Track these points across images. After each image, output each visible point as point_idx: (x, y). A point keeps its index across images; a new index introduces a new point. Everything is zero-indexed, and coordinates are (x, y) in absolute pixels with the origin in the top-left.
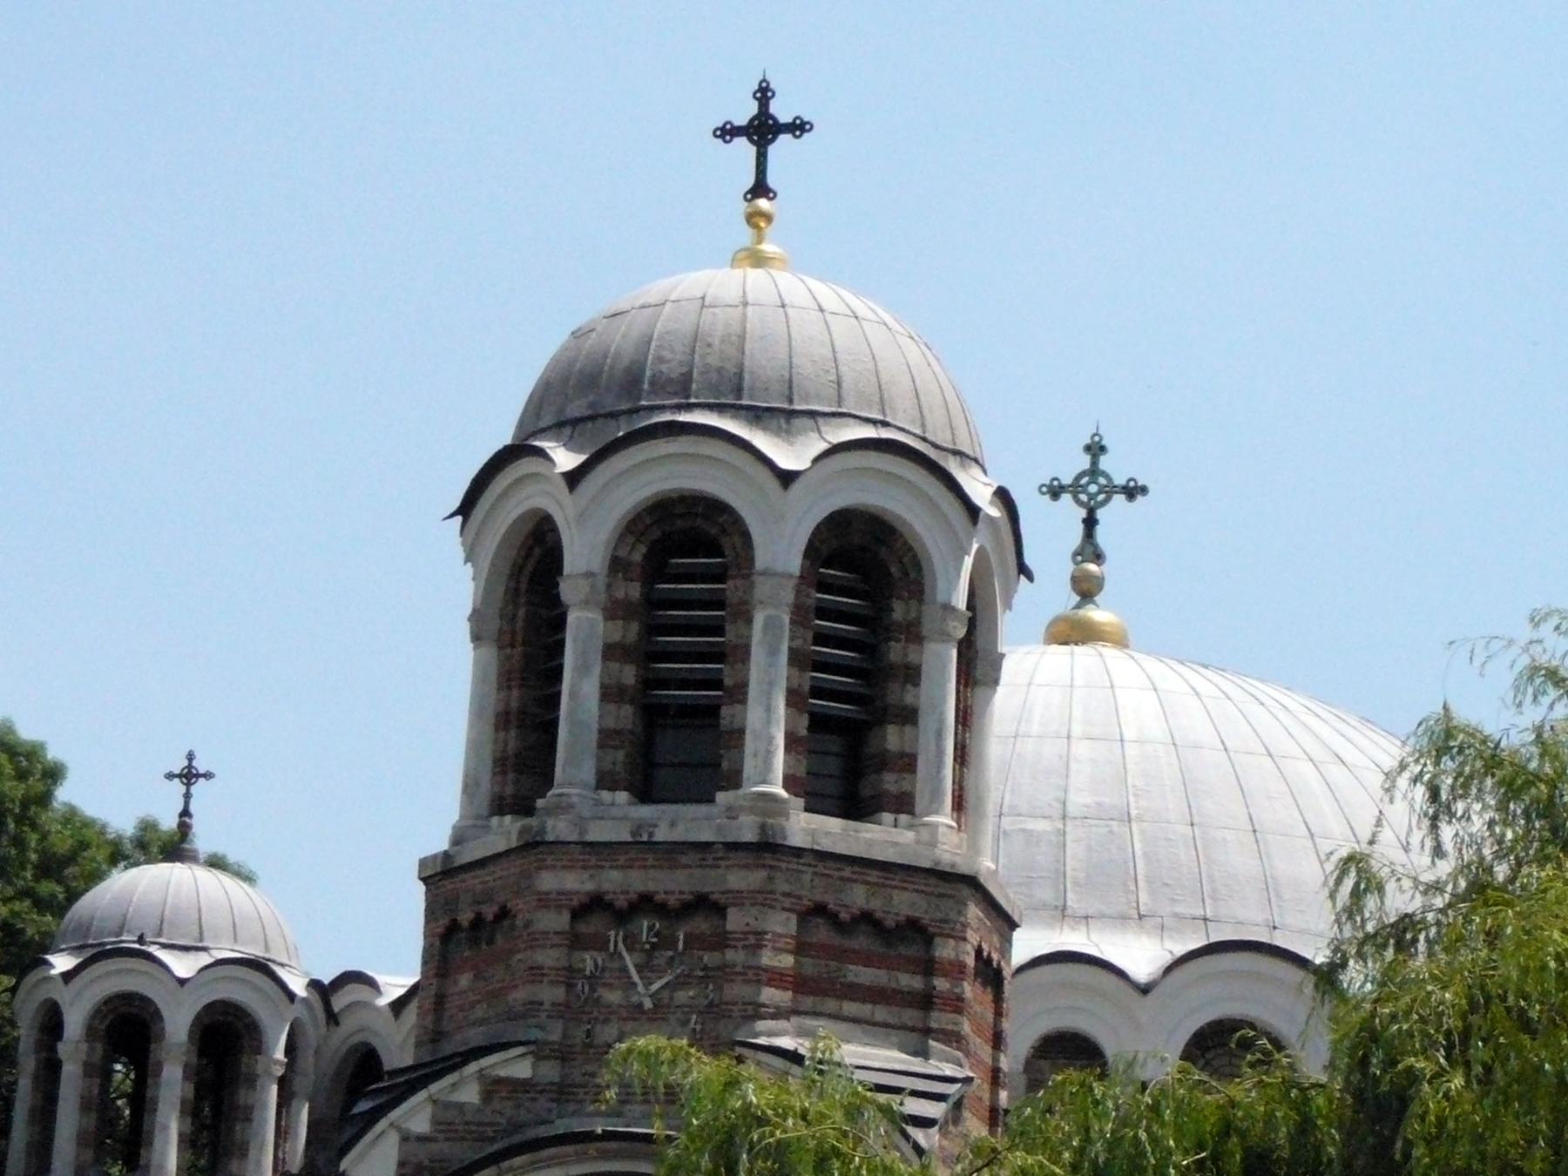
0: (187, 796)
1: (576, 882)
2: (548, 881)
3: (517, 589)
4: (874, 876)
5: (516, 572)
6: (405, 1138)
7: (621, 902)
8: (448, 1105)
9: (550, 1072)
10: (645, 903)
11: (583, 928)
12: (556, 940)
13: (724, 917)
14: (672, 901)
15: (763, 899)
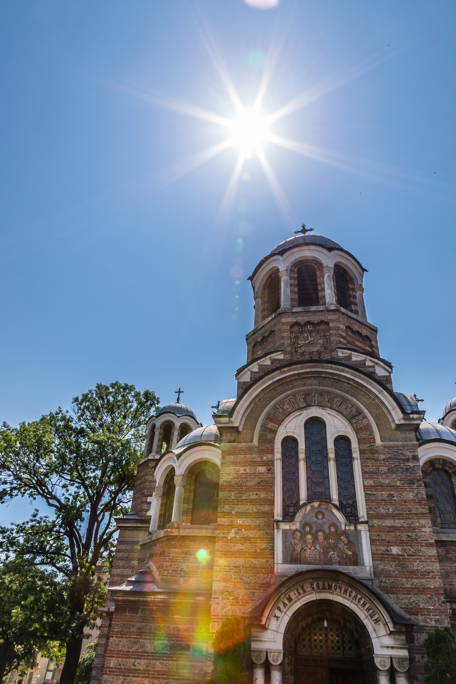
0: (179, 395)
1: (291, 320)
2: (284, 320)
3: (266, 284)
4: (359, 324)
5: (265, 285)
6: (252, 373)
7: (302, 323)
8: (262, 365)
9: (288, 357)
10: (309, 323)
12: (287, 331)
13: (329, 325)
14: (315, 322)
15: (338, 321)
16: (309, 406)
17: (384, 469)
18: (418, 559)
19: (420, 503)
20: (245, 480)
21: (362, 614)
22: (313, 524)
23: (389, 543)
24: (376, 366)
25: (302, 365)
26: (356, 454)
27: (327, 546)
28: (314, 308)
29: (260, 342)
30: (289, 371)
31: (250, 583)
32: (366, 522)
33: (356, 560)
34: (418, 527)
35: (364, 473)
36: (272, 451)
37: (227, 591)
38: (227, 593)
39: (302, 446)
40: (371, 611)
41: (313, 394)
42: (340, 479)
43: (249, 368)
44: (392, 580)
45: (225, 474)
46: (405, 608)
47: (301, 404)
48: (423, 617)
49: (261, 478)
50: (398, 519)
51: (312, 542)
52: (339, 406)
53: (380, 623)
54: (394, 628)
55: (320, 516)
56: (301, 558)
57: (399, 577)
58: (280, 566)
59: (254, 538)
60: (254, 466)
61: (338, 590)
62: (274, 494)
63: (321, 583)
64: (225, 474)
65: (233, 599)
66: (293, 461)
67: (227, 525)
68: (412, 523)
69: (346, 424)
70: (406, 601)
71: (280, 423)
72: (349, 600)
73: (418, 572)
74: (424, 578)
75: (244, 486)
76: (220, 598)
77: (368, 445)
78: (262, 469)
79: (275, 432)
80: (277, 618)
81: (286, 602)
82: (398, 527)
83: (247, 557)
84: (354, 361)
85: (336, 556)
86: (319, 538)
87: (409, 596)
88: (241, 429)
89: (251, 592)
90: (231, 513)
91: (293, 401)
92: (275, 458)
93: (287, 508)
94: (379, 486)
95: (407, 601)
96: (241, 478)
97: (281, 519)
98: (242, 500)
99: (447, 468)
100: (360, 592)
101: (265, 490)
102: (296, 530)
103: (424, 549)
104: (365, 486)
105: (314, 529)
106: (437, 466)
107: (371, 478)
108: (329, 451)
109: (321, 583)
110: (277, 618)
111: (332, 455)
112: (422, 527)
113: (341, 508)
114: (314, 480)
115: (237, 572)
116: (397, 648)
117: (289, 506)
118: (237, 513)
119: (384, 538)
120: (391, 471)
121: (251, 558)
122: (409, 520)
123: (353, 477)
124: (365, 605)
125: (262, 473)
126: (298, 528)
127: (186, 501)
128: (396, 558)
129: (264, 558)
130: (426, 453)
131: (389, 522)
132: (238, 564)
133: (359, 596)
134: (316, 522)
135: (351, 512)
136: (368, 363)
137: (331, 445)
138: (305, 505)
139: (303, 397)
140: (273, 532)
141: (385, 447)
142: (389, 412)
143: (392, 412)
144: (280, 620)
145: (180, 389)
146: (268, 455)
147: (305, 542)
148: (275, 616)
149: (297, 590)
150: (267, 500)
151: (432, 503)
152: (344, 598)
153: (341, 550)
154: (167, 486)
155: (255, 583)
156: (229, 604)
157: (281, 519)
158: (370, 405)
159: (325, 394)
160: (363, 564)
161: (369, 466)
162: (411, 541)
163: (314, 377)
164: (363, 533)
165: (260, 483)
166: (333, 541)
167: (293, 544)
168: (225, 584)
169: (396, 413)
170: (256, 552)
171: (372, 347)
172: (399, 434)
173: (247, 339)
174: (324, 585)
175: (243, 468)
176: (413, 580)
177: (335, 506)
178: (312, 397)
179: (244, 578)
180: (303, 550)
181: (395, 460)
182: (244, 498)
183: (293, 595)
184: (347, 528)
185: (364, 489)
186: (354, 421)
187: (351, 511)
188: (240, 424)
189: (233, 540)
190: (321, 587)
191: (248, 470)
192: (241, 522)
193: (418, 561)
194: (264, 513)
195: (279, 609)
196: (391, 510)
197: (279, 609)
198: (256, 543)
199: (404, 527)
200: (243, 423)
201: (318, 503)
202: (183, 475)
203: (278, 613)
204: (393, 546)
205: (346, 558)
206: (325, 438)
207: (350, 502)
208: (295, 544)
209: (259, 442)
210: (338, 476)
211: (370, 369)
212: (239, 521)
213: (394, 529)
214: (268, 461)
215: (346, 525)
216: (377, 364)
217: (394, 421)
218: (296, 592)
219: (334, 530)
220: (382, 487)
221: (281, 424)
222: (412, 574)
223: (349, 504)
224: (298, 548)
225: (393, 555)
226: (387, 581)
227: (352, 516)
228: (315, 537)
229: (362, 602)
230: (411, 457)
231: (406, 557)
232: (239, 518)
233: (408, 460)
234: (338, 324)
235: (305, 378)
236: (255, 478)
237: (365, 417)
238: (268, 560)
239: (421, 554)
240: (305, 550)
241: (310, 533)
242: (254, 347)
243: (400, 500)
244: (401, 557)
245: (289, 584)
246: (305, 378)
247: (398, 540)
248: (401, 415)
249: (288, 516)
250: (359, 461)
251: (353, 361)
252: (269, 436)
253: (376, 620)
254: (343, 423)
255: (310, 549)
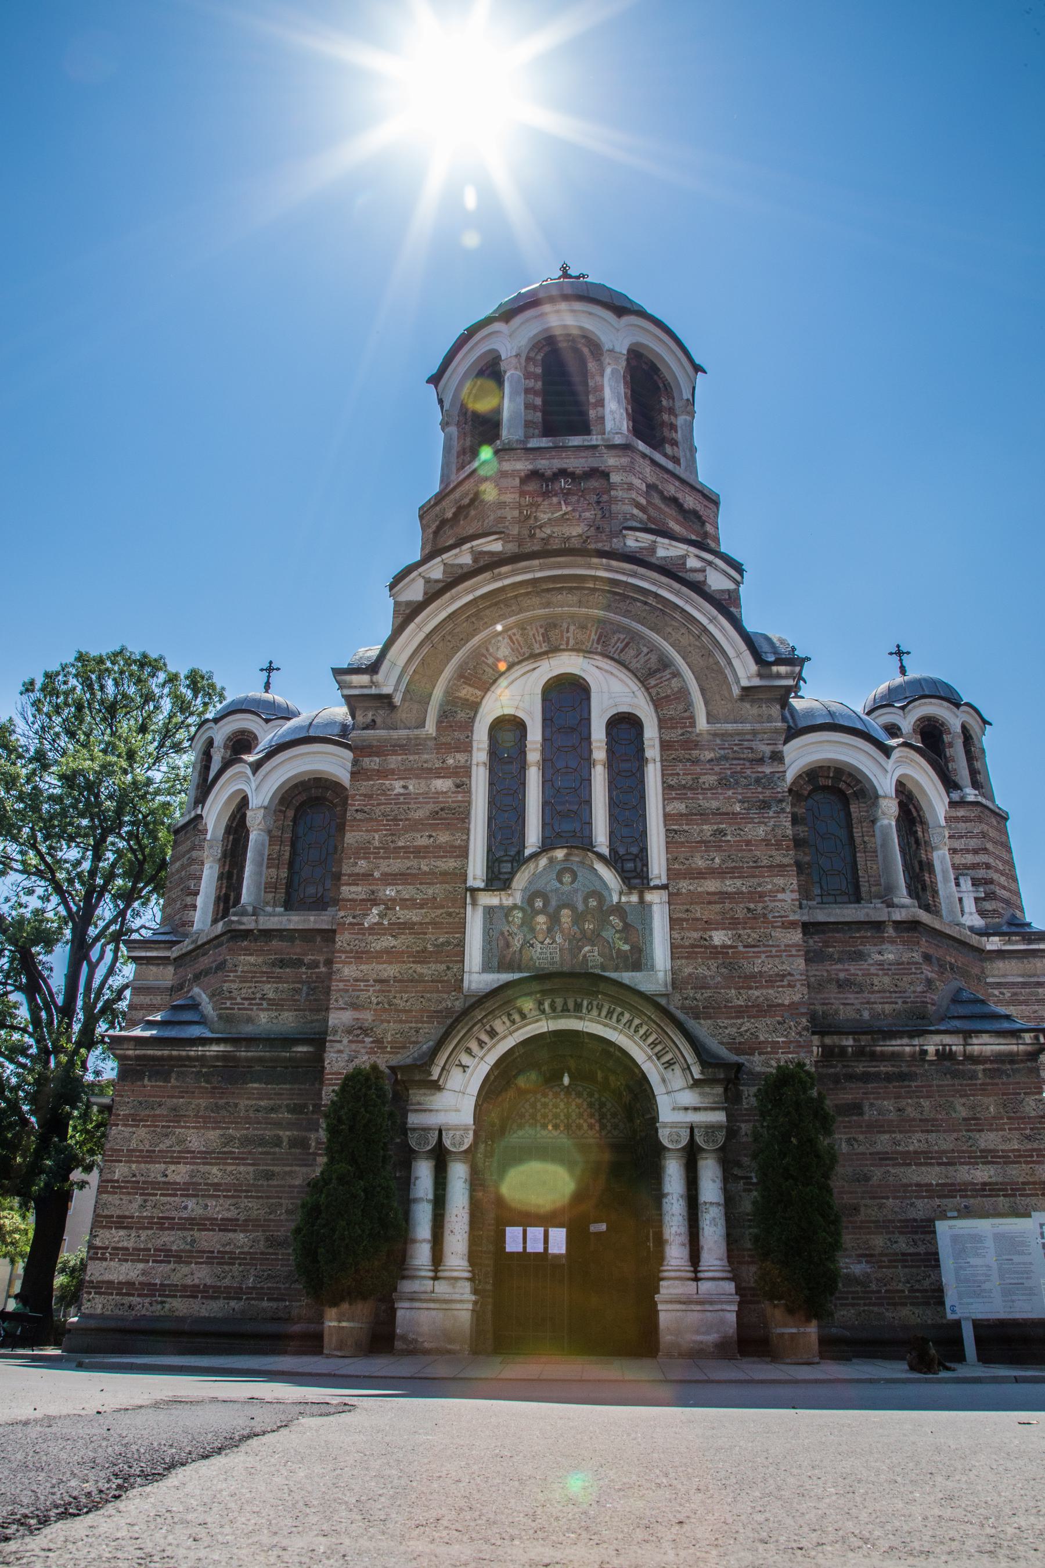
0: (269, 677)
4: (677, 483)
6: (428, 581)
7: (549, 473)
8: (452, 565)
10: (563, 473)
11: (526, 488)
13: (608, 480)
14: (578, 471)
15: (629, 469)
16: (554, 650)
17: (711, 779)
18: (764, 952)
19: (778, 845)
20: (405, 807)
21: (639, 1053)
22: (550, 895)
23: (709, 925)
24: (708, 568)
25: (541, 561)
26: (652, 751)
27: (578, 936)
28: (576, 441)
29: (452, 519)
30: (514, 573)
31: (410, 1011)
32: (665, 887)
33: (638, 960)
34: (771, 891)
35: (667, 787)
36: (466, 747)
37: (361, 1028)
38: (359, 1032)
39: (535, 735)
40: (659, 1048)
41: (565, 625)
42: (614, 804)
43: (421, 570)
44: (708, 993)
45: (360, 795)
46: (729, 1043)
47: (536, 646)
48: (763, 1057)
49: (442, 802)
50: (731, 878)
51: (548, 928)
52: (622, 651)
53: (676, 1067)
54: (702, 1073)
55: (567, 878)
56: (521, 960)
57: (724, 988)
58: (475, 977)
59: (421, 924)
60: (425, 778)
61: (595, 1012)
62: (468, 834)
63: (559, 1002)
64: (360, 795)
65: (372, 1042)
66: (514, 768)
67: (362, 900)
68: (759, 885)
69: (635, 688)
70: (733, 1031)
71: (487, 686)
72: (615, 1029)
73: (761, 976)
74: (773, 987)
75: (401, 820)
76: (345, 1041)
77: (680, 732)
78: (442, 785)
79: (474, 707)
80: (464, 1068)
81: (484, 1037)
82: (730, 893)
83: (404, 962)
84: (661, 558)
85: (596, 954)
86: (563, 920)
87: (739, 1021)
88: (397, 700)
89: (411, 1028)
90: (372, 875)
91: (520, 639)
92: (474, 762)
93: (496, 864)
94: (696, 815)
95: (735, 1030)
96: (396, 804)
97: (482, 885)
98: (395, 848)
99: (843, 786)
100: (640, 1013)
101: (448, 827)
102: (515, 907)
103: (777, 933)
104: (666, 816)
105: (554, 903)
106: (822, 782)
107: (680, 798)
108: (594, 745)
109: (559, 1002)
110: (464, 1068)
111: (599, 754)
112: (778, 891)
113: (614, 861)
114: (559, 808)
115: (383, 991)
116: (706, 1109)
117: (499, 861)
118: (385, 875)
119: (698, 915)
120: (723, 783)
121: (414, 962)
122: (752, 880)
123: (642, 798)
124: (647, 1037)
125: (442, 793)
126: (519, 902)
127: (273, 862)
128: (720, 953)
129: (441, 963)
130: (801, 755)
131: (711, 885)
132: (385, 975)
133: (637, 1021)
134: (557, 890)
135: (635, 870)
136: (692, 563)
137: (598, 734)
138: (534, 856)
139: (542, 631)
140: (462, 911)
141: (715, 735)
142: (730, 663)
143: (736, 663)
144: (469, 1071)
145: (271, 663)
146: (458, 756)
147: (532, 930)
148: (461, 1065)
149: (509, 1015)
150: (452, 846)
151: (805, 854)
152: (606, 1025)
153: (608, 942)
154: (231, 837)
155: (422, 1010)
156: (363, 1051)
157: (482, 885)
158: (690, 649)
159: (592, 626)
160: (652, 968)
161: (678, 774)
162: (754, 918)
163: (571, 589)
164: (656, 909)
165: (437, 813)
166: (591, 927)
167: (506, 933)
168: (357, 1015)
169: (745, 666)
170: (424, 950)
171: (706, 535)
172: (749, 709)
173: (421, 517)
174: (565, 1004)
175: (402, 783)
176: (750, 992)
177: (600, 857)
178: (562, 632)
179: (397, 1001)
180: (528, 944)
181: (735, 762)
182: (400, 844)
183: (499, 1026)
184: (624, 899)
185: (665, 821)
186: (653, 682)
187: (635, 867)
188: (396, 690)
189: (376, 930)
190: (559, 1009)
191: (411, 787)
192: (393, 894)
193: (763, 956)
194: (444, 874)
195: (469, 1051)
196: (717, 860)
197: (469, 1051)
198: (425, 934)
199: (742, 893)
200: (402, 687)
201: (565, 851)
202: (265, 808)
203: (465, 1059)
204: (716, 929)
205: (617, 958)
206: (586, 721)
207: (634, 850)
208: (510, 934)
209: (438, 728)
210: (611, 798)
211: (696, 574)
212: (390, 892)
213: (723, 896)
214: (456, 767)
215: (621, 893)
216: (710, 563)
217: (738, 681)
218: (505, 1019)
219: (595, 903)
220: (703, 815)
221: (488, 689)
222: (750, 980)
223: (630, 854)
224: (516, 943)
225: (716, 947)
226: (698, 996)
227: (634, 878)
228: (554, 919)
229: (642, 1032)
230: (768, 754)
231: (741, 949)
232: (389, 884)
233: (761, 761)
234: (631, 480)
235: (548, 590)
236: (428, 803)
237: (677, 674)
238: (451, 966)
239: (771, 943)
240: (532, 945)
241: (543, 911)
242: (436, 533)
243: (739, 841)
244: (730, 951)
245: (490, 1005)
246: (548, 590)
247: (727, 919)
248: (753, 668)
249: (498, 878)
250: (658, 764)
251: (658, 558)
252: (461, 716)
253: (667, 1062)
254: (627, 685)
255: (542, 943)
